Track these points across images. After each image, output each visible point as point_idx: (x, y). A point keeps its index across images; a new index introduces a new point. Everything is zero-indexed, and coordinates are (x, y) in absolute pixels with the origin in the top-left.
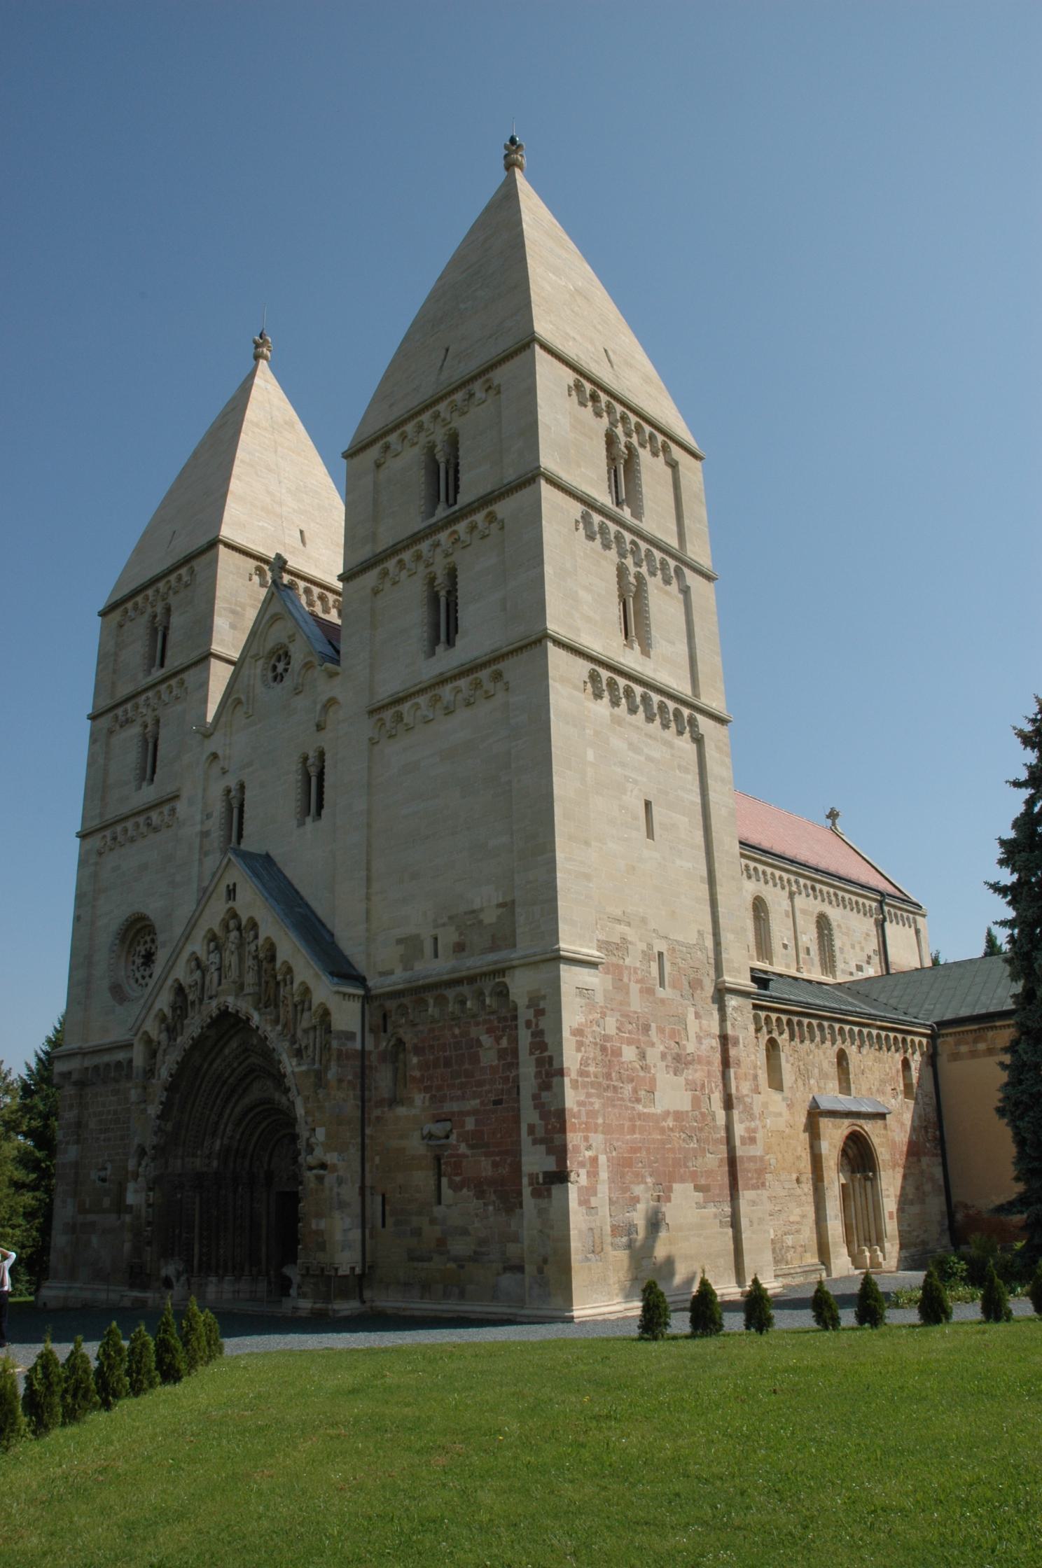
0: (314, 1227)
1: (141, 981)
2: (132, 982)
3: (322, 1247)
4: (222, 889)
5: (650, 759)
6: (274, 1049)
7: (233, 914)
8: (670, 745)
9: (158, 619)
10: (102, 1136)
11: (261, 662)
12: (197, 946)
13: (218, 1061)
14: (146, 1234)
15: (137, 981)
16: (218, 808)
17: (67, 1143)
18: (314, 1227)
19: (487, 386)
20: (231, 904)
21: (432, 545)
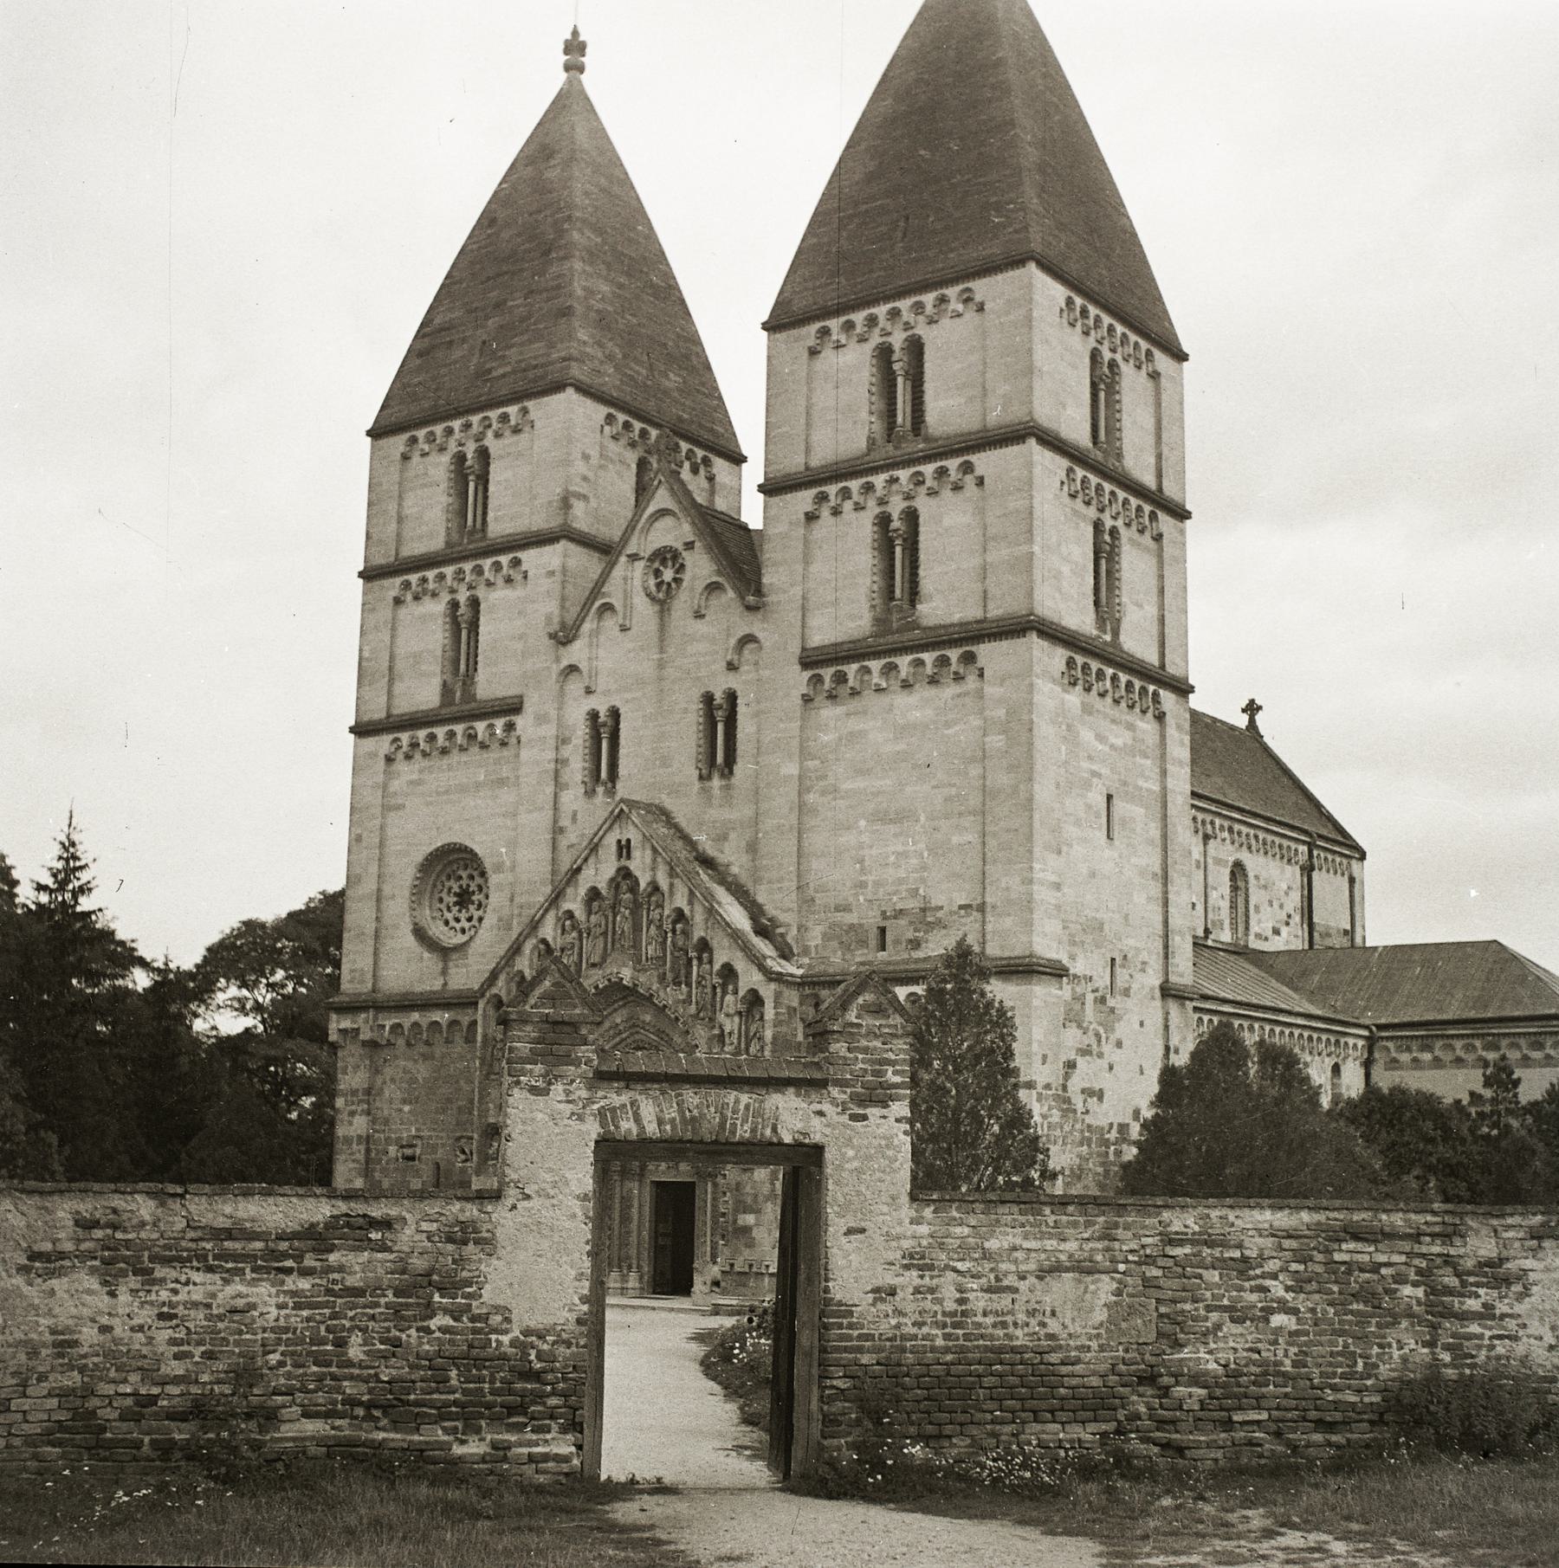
1: (452, 923)
2: (440, 923)
4: (611, 840)
5: (1112, 746)
7: (625, 874)
8: (1131, 727)
9: (469, 463)
11: (640, 565)
12: (574, 903)
15: (447, 923)
16: (581, 732)
17: (352, 1114)
19: (965, 296)
20: (624, 862)
21: (887, 481)
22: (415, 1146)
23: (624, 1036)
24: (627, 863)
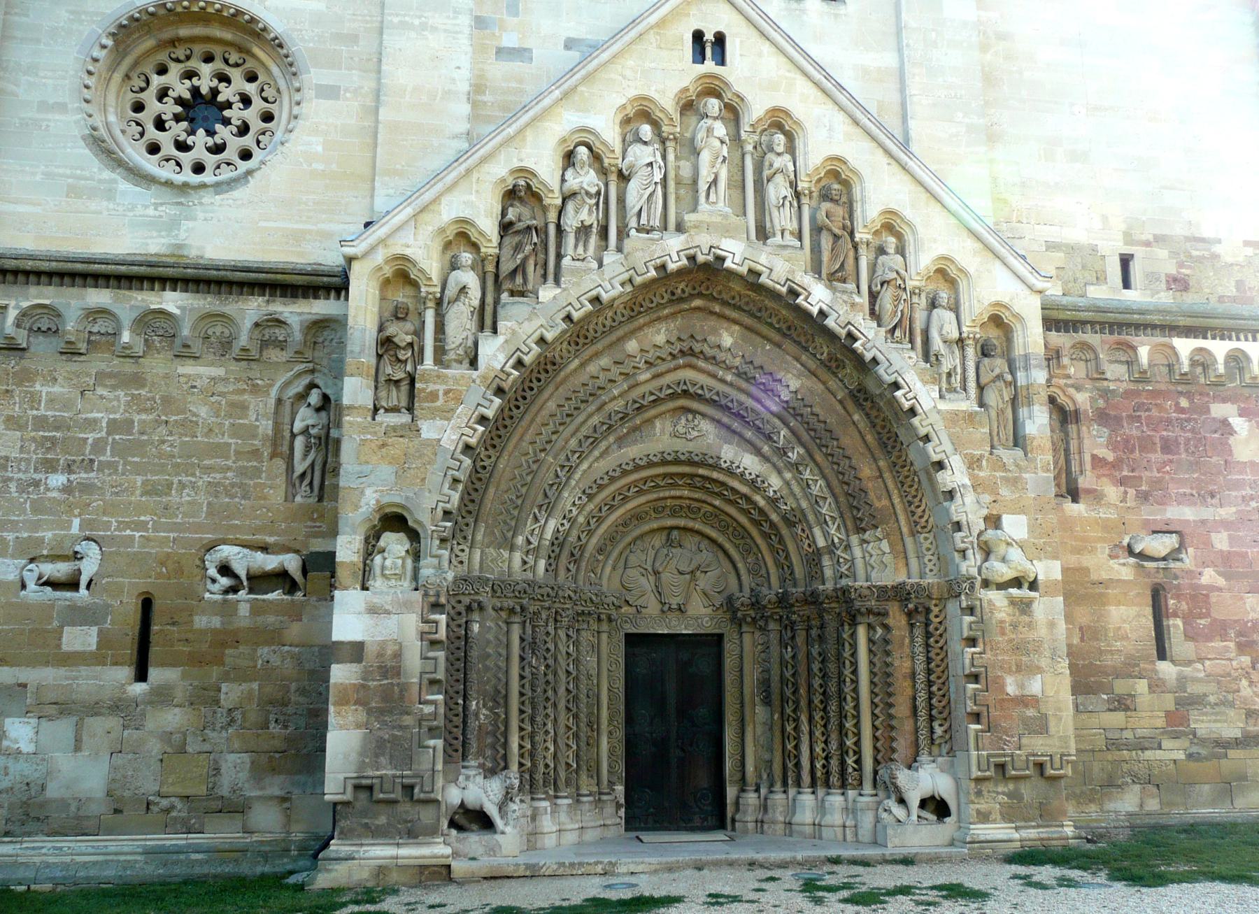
0: (1011, 689)
3: (1041, 726)
6: (875, 361)
7: (713, 89)
10: (58, 480)
13: (605, 361)
14: (428, 709)
18: (1011, 689)
20: (709, 66)
22: (77, 556)
23: (663, 367)
24: (719, 70)
